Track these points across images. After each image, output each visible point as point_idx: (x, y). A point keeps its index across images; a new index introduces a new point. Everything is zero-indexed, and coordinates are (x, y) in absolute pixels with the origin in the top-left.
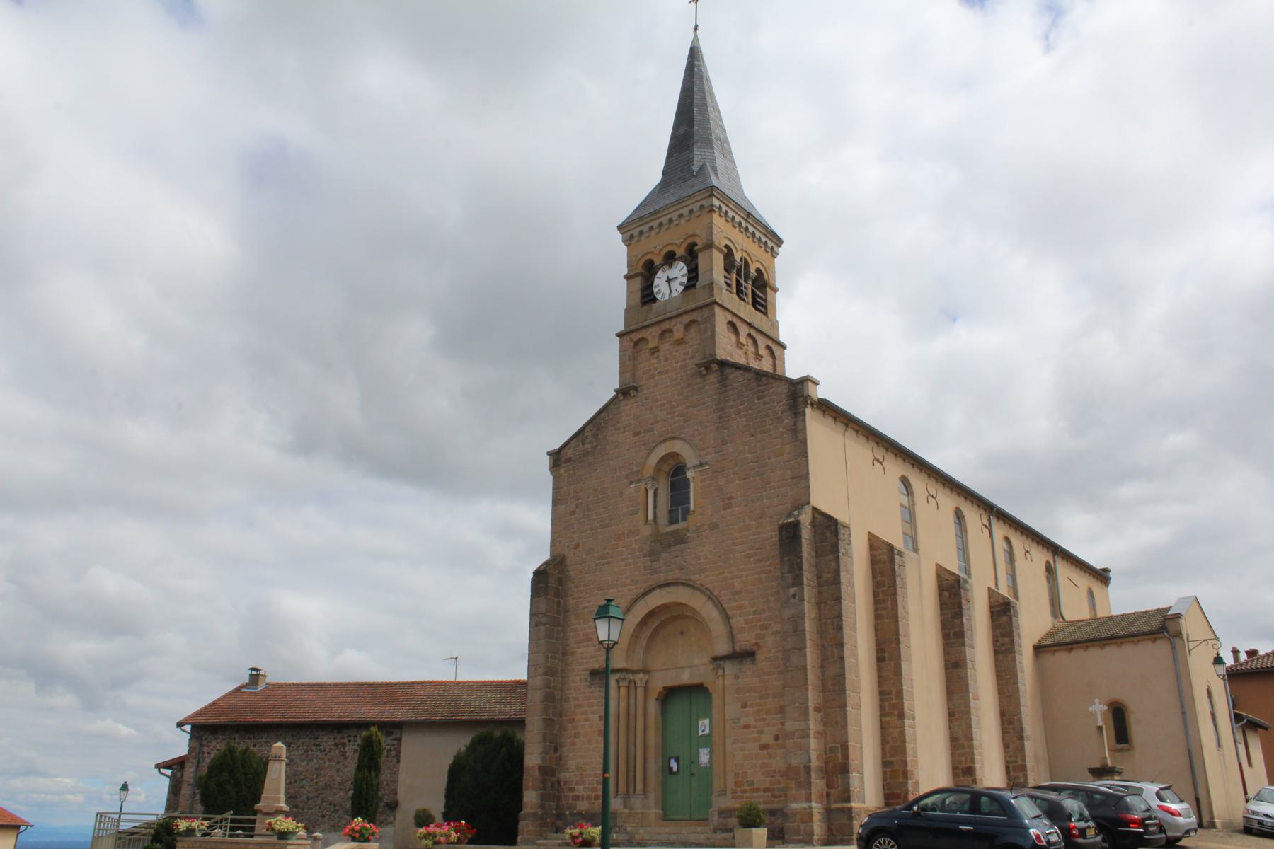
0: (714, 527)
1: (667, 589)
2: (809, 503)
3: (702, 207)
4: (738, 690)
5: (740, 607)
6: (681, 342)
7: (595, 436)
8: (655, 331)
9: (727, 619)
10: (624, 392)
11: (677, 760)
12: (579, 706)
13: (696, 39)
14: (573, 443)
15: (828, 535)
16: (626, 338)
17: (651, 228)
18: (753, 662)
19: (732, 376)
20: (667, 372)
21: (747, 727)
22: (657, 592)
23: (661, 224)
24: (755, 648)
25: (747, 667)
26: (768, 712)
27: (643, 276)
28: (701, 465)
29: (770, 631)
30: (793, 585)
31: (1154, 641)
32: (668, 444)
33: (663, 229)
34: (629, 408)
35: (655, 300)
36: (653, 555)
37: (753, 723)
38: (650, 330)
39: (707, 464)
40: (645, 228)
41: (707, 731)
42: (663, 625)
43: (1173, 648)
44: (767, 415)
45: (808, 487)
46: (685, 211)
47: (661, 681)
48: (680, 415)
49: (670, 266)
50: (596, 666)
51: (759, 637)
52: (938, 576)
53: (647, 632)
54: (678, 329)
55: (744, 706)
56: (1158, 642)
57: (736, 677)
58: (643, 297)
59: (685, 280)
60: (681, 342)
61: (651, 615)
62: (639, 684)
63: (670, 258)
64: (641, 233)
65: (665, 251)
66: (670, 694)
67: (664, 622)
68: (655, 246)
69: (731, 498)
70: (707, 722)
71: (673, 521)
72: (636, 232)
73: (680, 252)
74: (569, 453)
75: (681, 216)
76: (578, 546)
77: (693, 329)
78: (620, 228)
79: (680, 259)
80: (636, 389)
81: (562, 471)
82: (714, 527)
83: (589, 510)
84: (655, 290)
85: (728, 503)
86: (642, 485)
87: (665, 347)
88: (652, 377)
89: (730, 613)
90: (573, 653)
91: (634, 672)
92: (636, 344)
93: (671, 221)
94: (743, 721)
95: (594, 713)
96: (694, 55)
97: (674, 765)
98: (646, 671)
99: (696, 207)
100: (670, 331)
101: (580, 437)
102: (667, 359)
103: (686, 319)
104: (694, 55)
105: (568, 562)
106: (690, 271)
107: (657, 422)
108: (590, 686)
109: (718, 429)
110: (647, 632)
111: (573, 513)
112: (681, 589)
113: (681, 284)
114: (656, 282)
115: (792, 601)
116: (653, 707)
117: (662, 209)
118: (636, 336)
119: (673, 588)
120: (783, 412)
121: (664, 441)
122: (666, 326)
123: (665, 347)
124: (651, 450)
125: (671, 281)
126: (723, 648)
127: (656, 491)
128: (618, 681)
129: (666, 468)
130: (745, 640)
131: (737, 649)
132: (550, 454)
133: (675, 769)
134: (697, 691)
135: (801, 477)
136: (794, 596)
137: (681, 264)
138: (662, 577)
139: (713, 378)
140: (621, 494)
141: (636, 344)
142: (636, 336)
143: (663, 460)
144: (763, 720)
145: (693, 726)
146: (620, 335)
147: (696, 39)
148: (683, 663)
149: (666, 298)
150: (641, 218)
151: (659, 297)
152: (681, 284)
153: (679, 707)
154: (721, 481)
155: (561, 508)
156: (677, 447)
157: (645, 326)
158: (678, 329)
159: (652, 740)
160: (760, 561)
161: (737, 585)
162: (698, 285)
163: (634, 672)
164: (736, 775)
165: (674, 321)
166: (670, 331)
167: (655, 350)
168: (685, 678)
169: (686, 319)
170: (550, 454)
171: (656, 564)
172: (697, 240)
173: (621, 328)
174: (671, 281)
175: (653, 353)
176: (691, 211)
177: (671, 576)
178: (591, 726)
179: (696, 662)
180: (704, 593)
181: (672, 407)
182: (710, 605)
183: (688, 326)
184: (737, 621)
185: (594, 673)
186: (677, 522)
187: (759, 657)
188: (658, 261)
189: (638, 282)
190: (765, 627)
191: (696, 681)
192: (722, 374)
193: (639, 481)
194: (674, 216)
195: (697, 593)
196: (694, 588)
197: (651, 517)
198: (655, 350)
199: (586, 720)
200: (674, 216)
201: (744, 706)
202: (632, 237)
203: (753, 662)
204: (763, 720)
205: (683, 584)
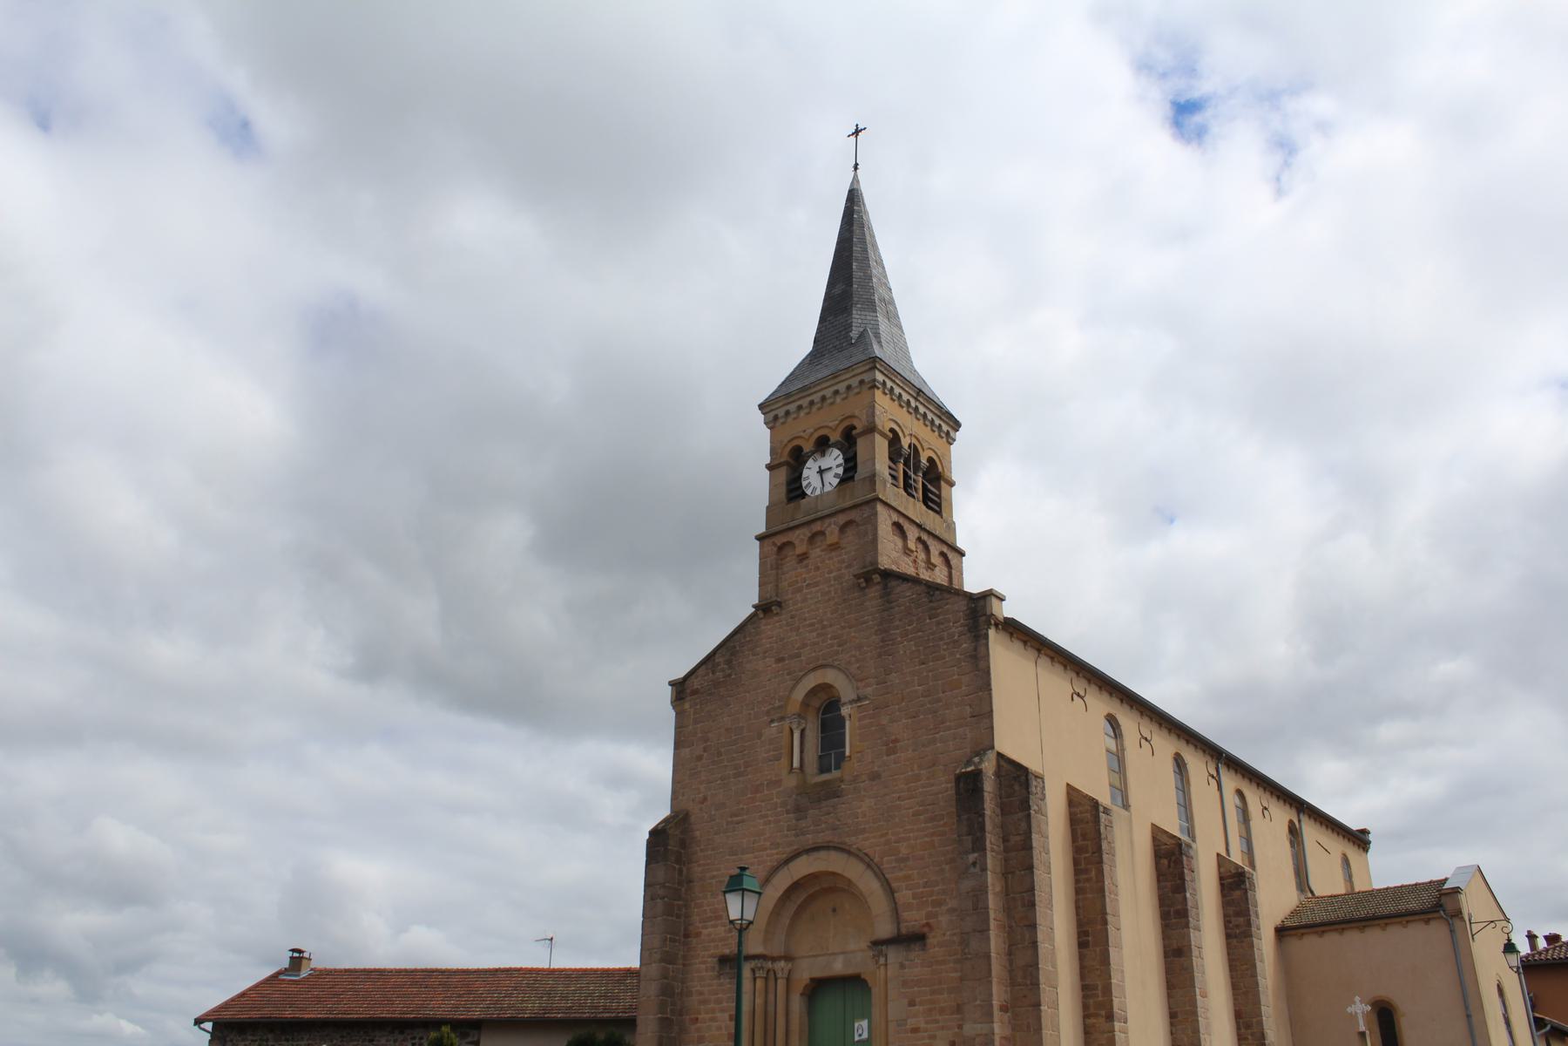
0: (875, 777)
1: (815, 855)
2: (993, 747)
3: (862, 382)
4: (905, 983)
5: (908, 878)
6: (834, 547)
7: (729, 662)
8: (805, 533)
9: (890, 891)
10: (765, 608)
12: (705, 1002)
13: (855, 179)
14: (700, 672)
15: (1017, 787)
16: (766, 542)
17: (800, 408)
18: (924, 947)
19: (899, 589)
20: (816, 584)
21: (915, 1030)
22: (804, 857)
23: (812, 403)
24: (926, 930)
25: (916, 954)
26: (942, 1011)
27: (789, 464)
28: (859, 699)
29: (944, 908)
30: (974, 851)
31: (1427, 922)
32: (819, 672)
33: (814, 409)
34: (771, 629)
35: (804, 495)
36: (799, 811)
37: (923, 1025)
38: (798, 532)
39: (866, 698)
40: (792, 407)
41: (865, 1036)
43: (1452, 931)
44: (941, 639)
45: (992, 728)
46: (842, 387)
47: (807, 971)
48: (833, 638)
49: (823, 454)
50: (727, 951)
51: (929, 915)
52: (1068, 793)
53: (791, 908)
54: (832, 530)
55: (912, 1004)
56: (1434, 925)
57: (902, 966)
58: (789, 491)
59: (840, 471)
60: (834, 547)
61: (795, 887)
62: (779, 975)
63: (822, 445)
64: (788, 413)
65: (816, 435)
66: (819, 987)
67: (813, 896)
68: (805, 428)
69: (896, 741)
70: (865, 1023)
71: (824, 769)
72: (781, 412)
73: (835, 437)
74: (695, 683)
75: (837, 392)
76: (705, 799)
77: (850, 532)
78: (761, 407)
79: (836, 445)
80: (779, 604)
81: (687, 706)
82: (875, 777)
83: (719, 754)
84: (804, 484)
85: (892, 747)
86: (786, 724)
87: (816, 553)
88: (800, 590)
89: (894, 885)
90: (698, 935)
91: (774, 959)
92: (781, 548)
93: (824, 398)
94: (911, 1023)
95: (722, 1010)
96: (854, 199)
98: (788, 958)
99: (854, 382)
100: (822, 533)
101: (710, 665)
102: (818, 568)
103: (842, 519)
104: (854, 199)
105: (692, 819)
106: (846, 460)
107: (805, 645)
108: (719, 976)
109: (880, 656)
110: (791, 908)
111: (700, 758)
112: (833, 854)
113: (836, 476)
114: (806, 473)
115: (972, 870)
116: (797, 1004)
117: (814, 384)
118: (780, 540)
119: (823, 854)
120: (961, 634)
121: (814, 669)
122: (817, 527)
123: (816, 553)
124: (798, 681)
125: (822, 475)
126: (885, 929)
127: (803, 731)
128: (753, 971)
129: (816, 703)
130: (914, 919)
131: (904, 931)
132: (672, 684)
134: (853, 983)
135: (983, 715)
136: (974, 864)
137: (836, 452)
138: (810, 839)
139: (874, 592)
140: (760, 736)
141: (781, 548)
142: (780, 540)
143: (813, 692)
144: (937, 1021)
145: (848, 1030)
146: (760, 538)
147: (855, 179)
148: (836, 949)
149: (818, 492)
150: (788, 395)
151: (808, 492)
152: (836, 476)
154: (885, 720)
155: (686, 752)
156: (830, 676)
157: (791, 526)
158: (832, 530)
160: (932, 819)
161: (904, 851)
162: (857, 477)
163: (774, 959)
165: (827, 521)
166: (822, 533)
167: (803, 557)
168: (838, 967)
169: (842, 519)
170: (672, 684)
171: (803, 824)
172: (855, 422)
173: (762, 529)
174: (822, 475)
175: (801, 561)
176: (849, 388)
177: (821, 839)
178: (719, 1028)
179: (852, 946)
180: (862, 860)
181: (824, 627)
182: (869, 874)
183: (843, 528)
184: (904, 895)
185: (723, 960)
186: (829, 770)
187: (931, 941)
188: (808, 447)
189: (783, 474)
190: (938, 903)
191: (850, 971)
192: (885, 587)
193: (782, 719)
194: (828, 393)
195: (853, 860)
196: (849, 852)
197: (796, 764)
198: (803, 557)
199: (713, 1019)
200: (828, 393)
201: (912, 1004)
202: (776, 418)
203: (924, 947)
204: (937, 1021)
205: (836, 848)
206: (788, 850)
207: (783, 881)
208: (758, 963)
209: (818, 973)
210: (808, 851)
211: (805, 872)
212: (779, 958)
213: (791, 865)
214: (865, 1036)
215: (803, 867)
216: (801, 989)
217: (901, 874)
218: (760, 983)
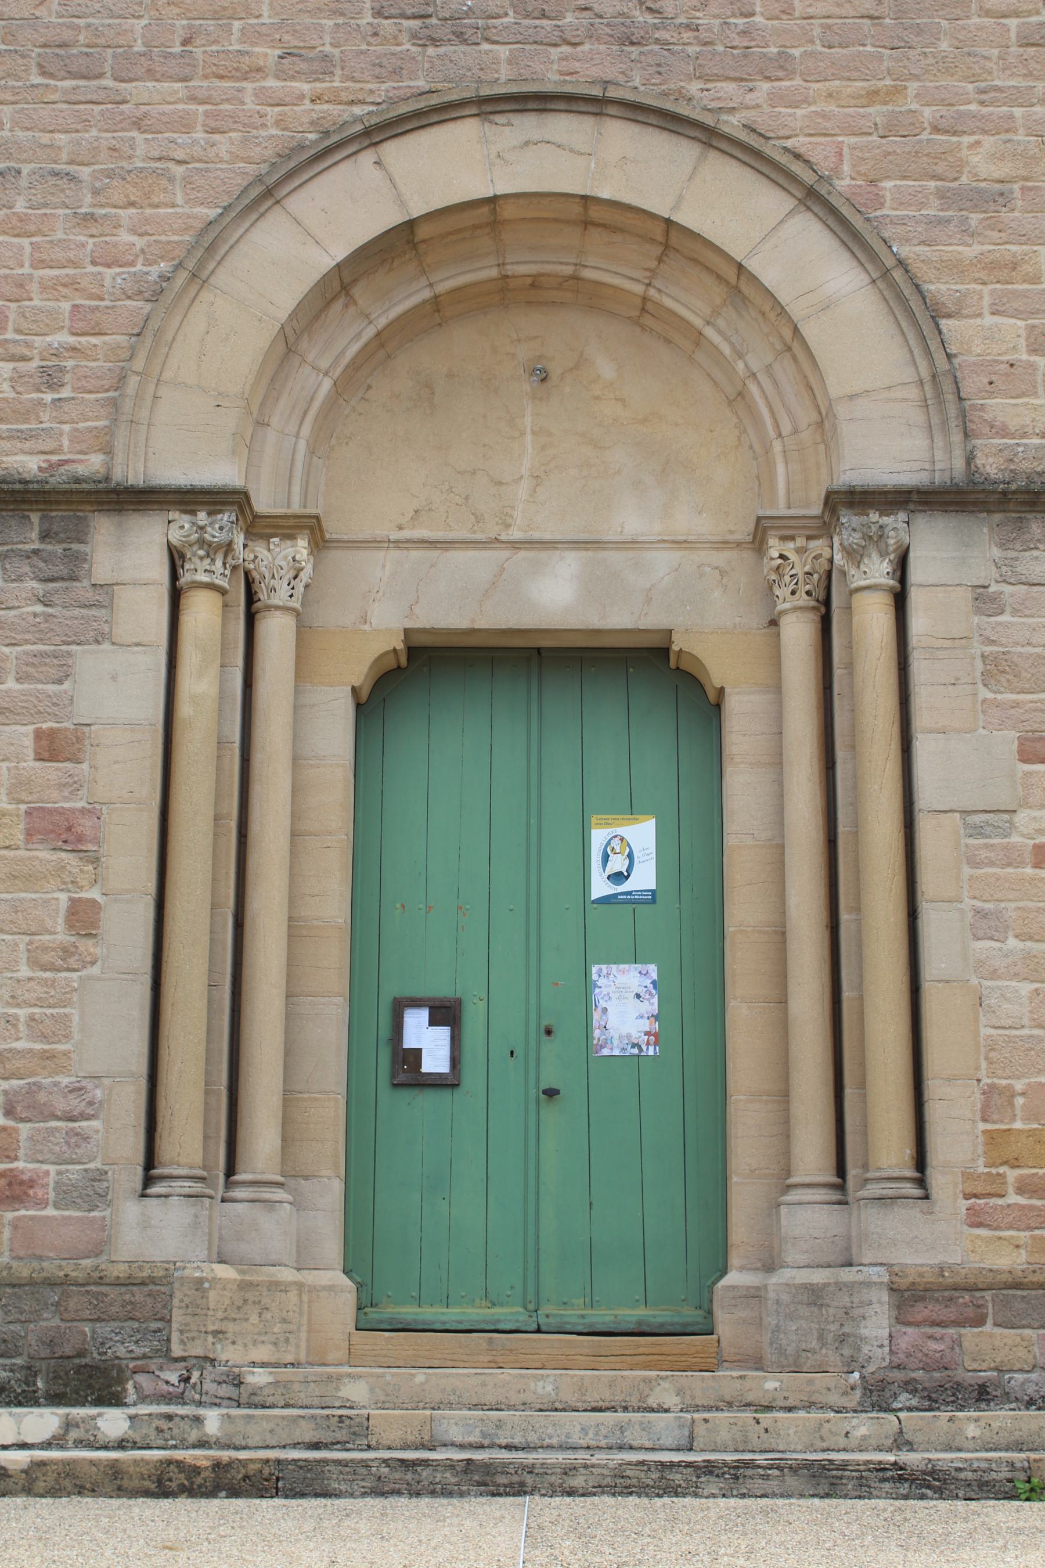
1: (528, 126)
4: (997, 669)
9: (915, 307)
11: (445, 1013)
22: (465, 132)
41: (644, 878)
42: (436, 313)
47: (384, 605)
53: (347, 337)
57: (984, 600)
61: (401, 244)
62: (277, 593)
66: (424, 670)
70: (642, 834)
89: (938, 287)
97: (429, 1042)
110: (347, 337)
112: (620, 137)
116: (313, 733)
119: (562, 127)
126: (890, 448)
128: (176, 559)
131: (991, 466)
133: (436, 1059)
134: (649, 671)
138: (500, 67)
145: (551, 851)
153: (463, 747)
159: (331, 903)
161: (982, 160)
164: (994, 1100)
168: (555, 598)
177: (550, 73)
179: (630, 520)
182: (809, 234)
191: (621, 617)
195: (725, 174)
196: (708, 136)
205: (637, 112)
206: (383, 89)
207: (349, 208)
208: (220, 526)
209: (457, 600)
210: (490, 106)
211: (475, 186)
212: (284, 527)
213: (393, 151)
214: (644, 878)
215: (450, 167)
216: (358, 672)
217: (970, 251)
218: (202, 614)
